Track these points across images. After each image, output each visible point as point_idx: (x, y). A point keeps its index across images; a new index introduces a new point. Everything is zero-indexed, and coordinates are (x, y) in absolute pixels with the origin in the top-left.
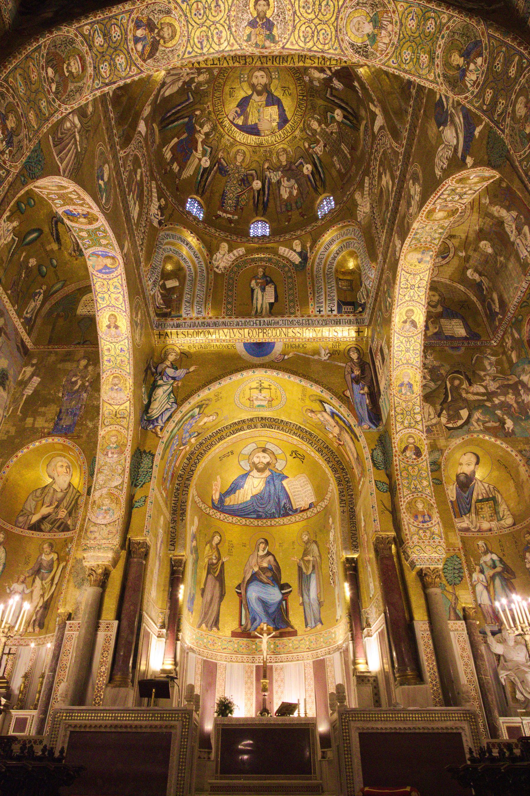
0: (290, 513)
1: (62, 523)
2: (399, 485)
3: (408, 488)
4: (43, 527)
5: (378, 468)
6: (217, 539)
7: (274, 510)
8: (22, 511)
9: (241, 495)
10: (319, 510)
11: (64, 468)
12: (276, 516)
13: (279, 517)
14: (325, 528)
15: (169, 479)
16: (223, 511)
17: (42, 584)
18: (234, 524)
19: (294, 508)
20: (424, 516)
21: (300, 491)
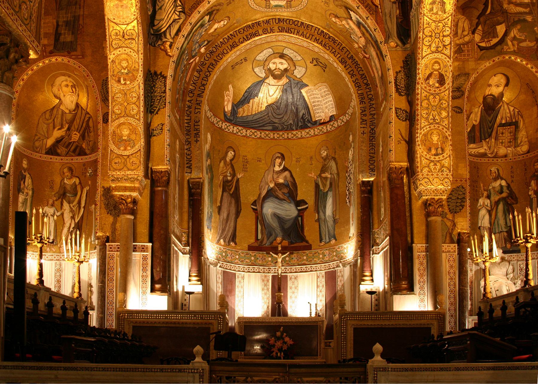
0: (309, 125)
1: (77, 147)
2: (418, 115)
3: (427, 119)
4: (59, 151)
5: (400, 95)
6: (231, 154)
7: (291, 122)
8: (36, 135)
9: (255, 106)
10: (339, 124)
11: (70, 87)
12: (294, 128)
13: (297, 129)
14: (345, 146)
15: (181, 98)
16: (236, 124)
17: (70, 206)
18: (248, 137)
19: (313, 120)
20: (437, 149)
21: (321, 101)
